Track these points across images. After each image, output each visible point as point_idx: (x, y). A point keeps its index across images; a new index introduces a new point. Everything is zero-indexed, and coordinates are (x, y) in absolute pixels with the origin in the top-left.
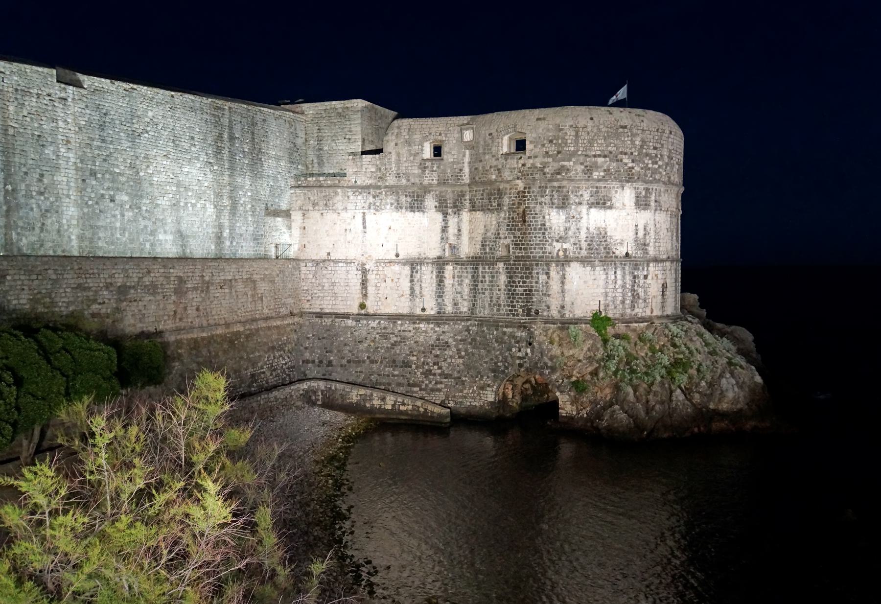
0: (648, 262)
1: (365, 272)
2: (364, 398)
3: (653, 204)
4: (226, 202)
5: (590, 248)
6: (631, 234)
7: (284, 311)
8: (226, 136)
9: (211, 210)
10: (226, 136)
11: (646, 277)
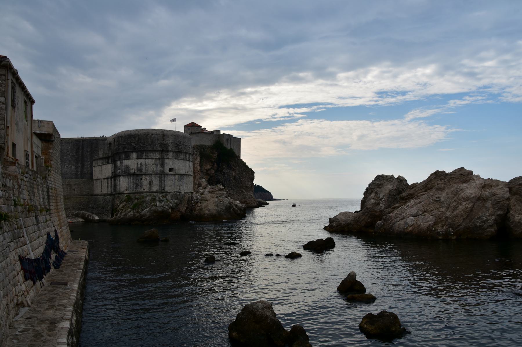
0: (142, 175)
1: (101, 181)
2: (88, 216)
3: (144, 157)
4: (79, 165)
5: (125, 171)
6: (135, 167)
7: (85, 193)
8: (80, 148)
9: (73, 167)
10: (80, 148)
11: (141, 179)
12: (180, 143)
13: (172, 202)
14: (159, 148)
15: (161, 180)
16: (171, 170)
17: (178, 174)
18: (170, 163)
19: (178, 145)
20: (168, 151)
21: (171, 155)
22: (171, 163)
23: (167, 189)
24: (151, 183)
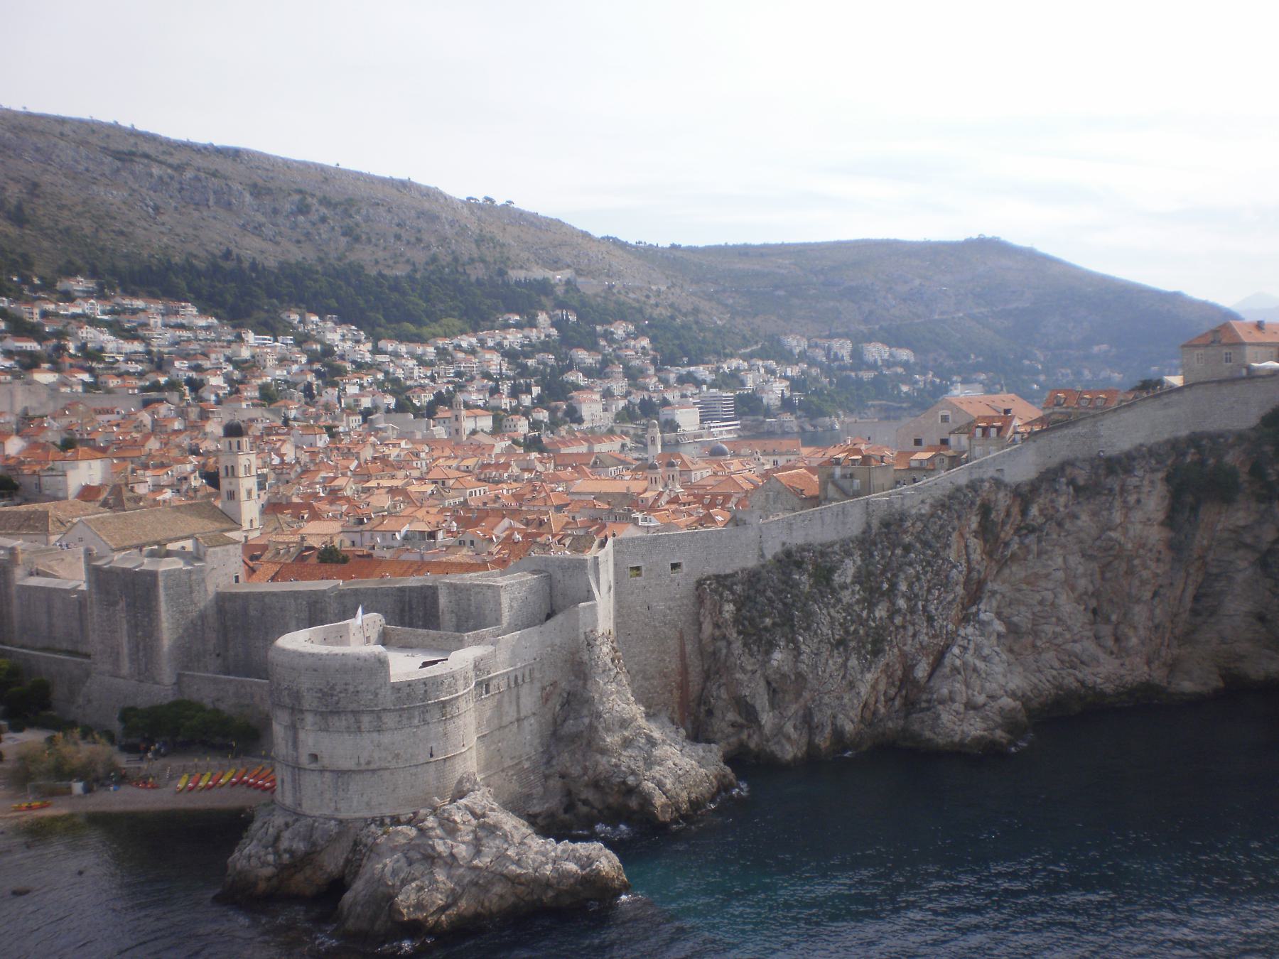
12: (332, 688)
13: (292, 842)
14: (287, 701)
15: (294, 780)
16: (314, 757)
17: (332, 771)
18: (310, 739)
19: (325, 694)
20: (302, 711)
21: (309, 718)
22: (311, 742)
23: (306, 807)
24: (283, 781)
